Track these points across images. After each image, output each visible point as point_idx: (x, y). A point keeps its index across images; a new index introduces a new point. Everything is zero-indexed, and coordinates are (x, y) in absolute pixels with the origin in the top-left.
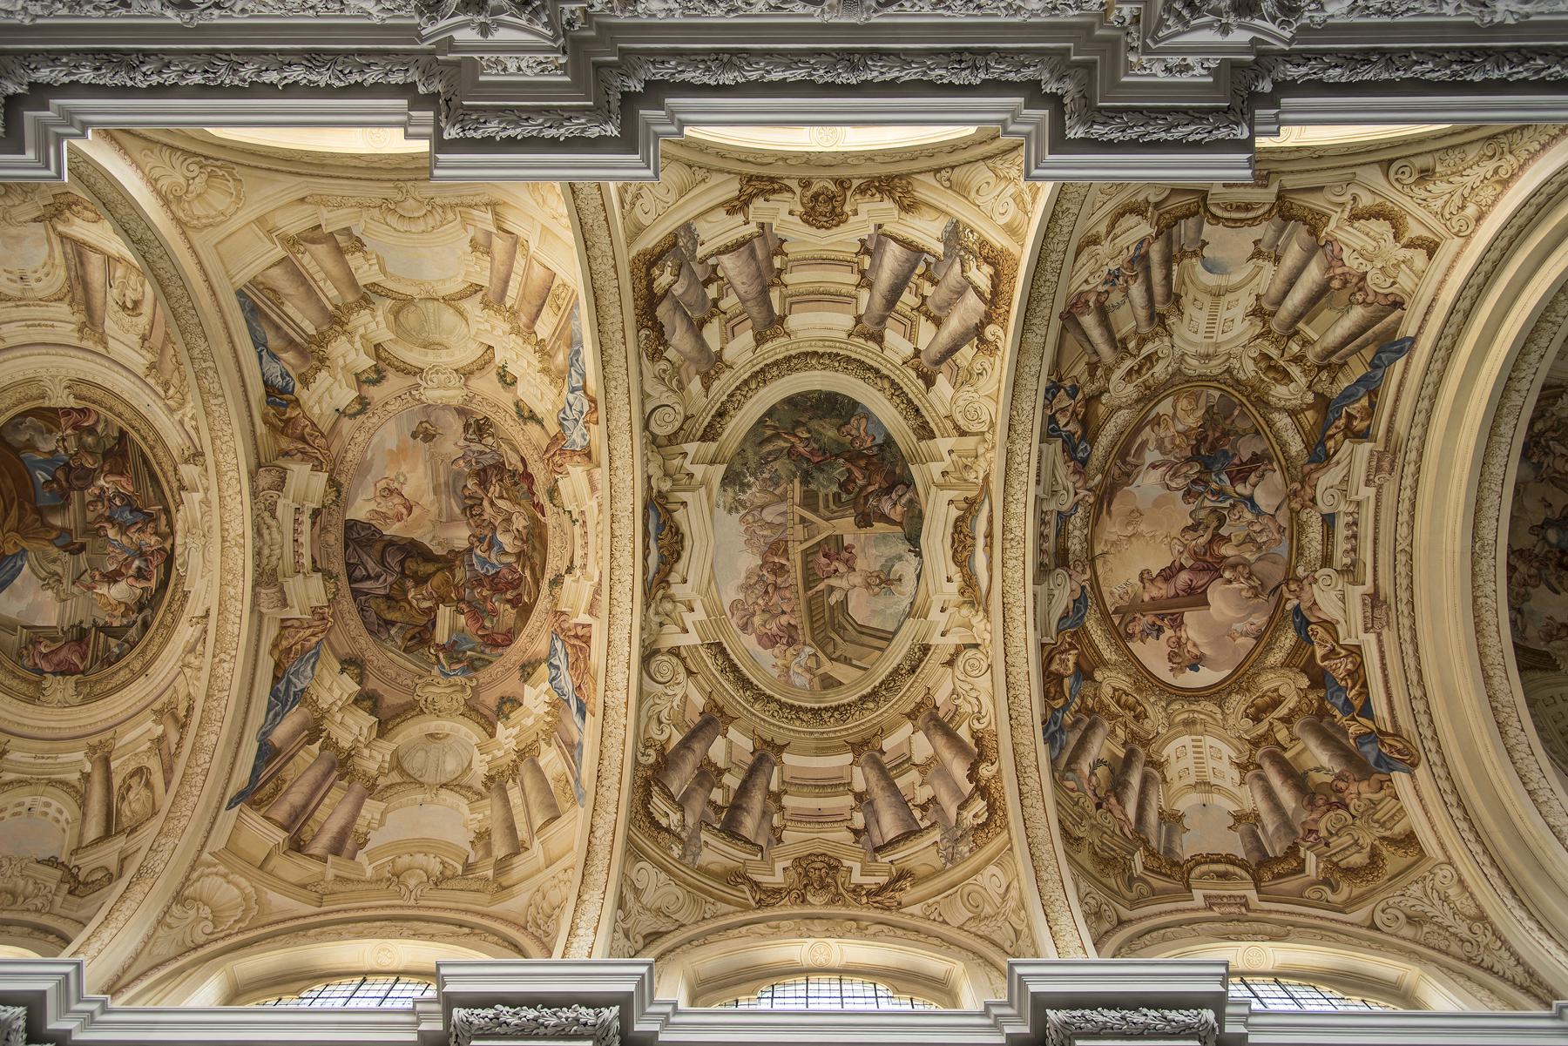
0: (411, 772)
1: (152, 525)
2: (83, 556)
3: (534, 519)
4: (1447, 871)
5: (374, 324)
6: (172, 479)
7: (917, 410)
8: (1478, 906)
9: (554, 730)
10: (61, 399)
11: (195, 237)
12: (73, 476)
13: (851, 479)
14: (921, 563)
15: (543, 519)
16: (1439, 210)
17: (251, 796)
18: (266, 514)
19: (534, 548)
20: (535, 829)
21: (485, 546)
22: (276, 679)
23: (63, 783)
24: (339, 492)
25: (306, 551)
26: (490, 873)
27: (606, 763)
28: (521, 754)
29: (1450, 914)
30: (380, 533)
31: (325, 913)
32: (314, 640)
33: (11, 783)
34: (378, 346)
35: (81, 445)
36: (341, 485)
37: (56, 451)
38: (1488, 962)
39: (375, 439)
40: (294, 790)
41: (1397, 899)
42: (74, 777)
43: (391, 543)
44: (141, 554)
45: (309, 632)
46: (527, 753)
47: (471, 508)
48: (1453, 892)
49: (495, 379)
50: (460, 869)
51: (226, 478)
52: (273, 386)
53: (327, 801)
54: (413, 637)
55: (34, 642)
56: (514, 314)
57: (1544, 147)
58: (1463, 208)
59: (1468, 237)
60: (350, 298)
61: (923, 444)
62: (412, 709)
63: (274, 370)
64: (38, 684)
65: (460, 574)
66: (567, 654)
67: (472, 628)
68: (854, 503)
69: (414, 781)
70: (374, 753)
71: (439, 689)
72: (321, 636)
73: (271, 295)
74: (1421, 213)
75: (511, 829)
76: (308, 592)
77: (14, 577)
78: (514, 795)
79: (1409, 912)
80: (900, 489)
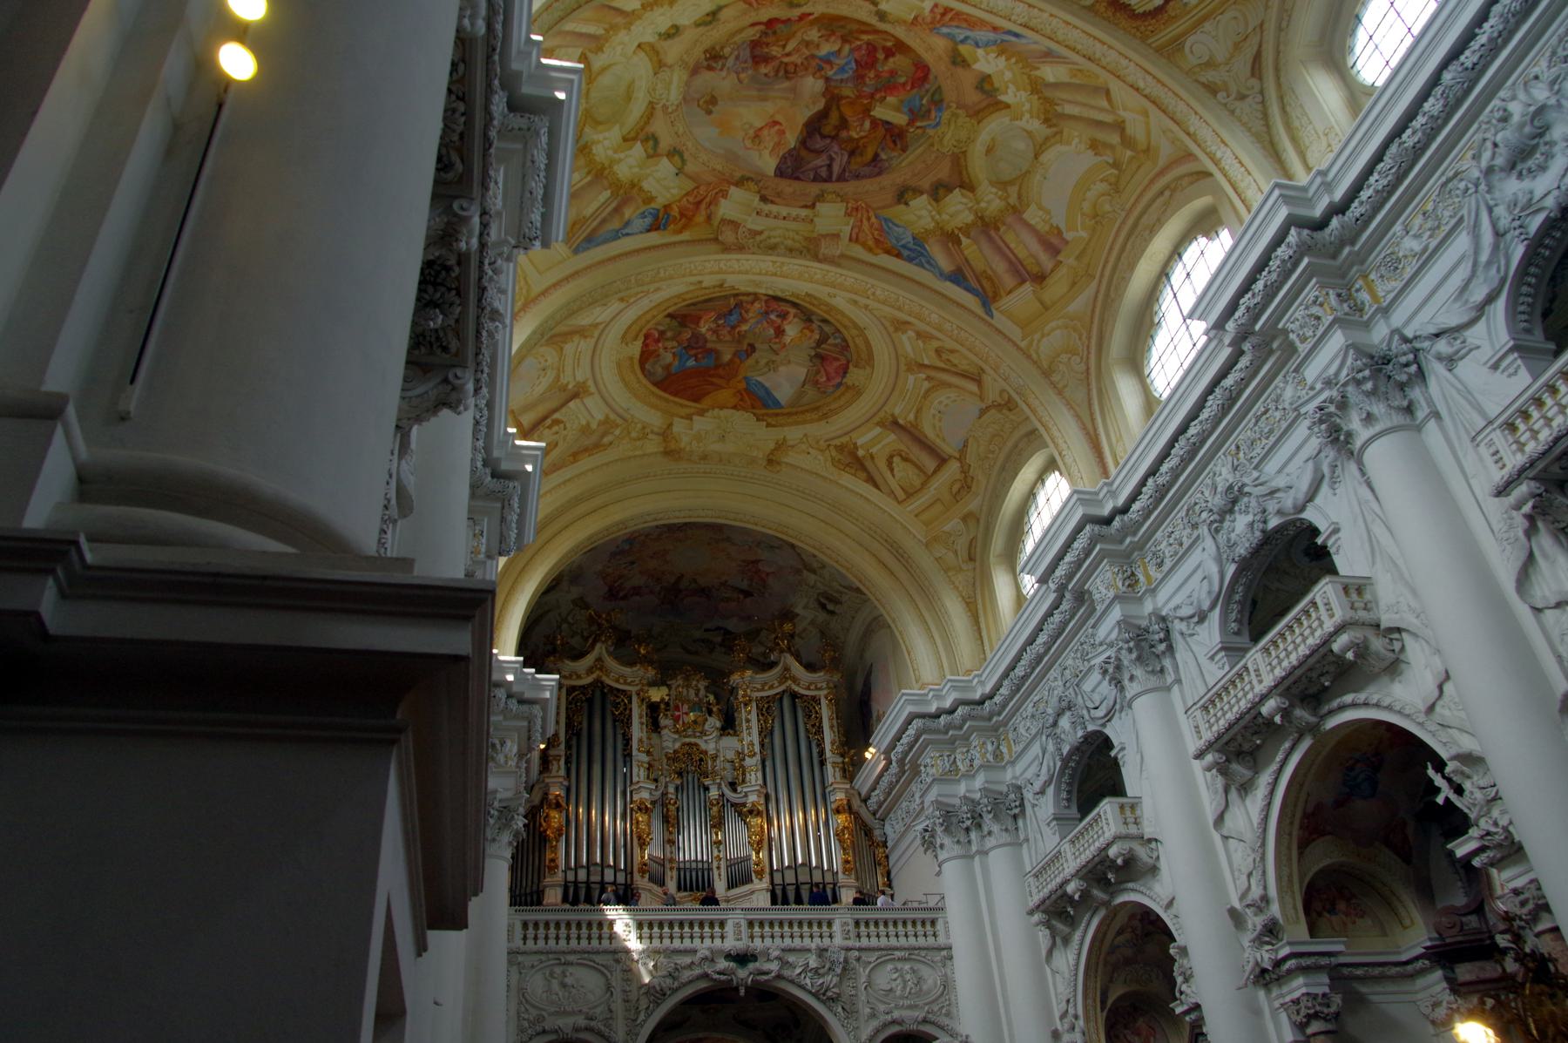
1: (744, 305)
2: (756, 345)
3: (812, 23)
6: (712, 290)
9: (1028, 62)
10: (636, 348)
11: (536, 290)
12: (696, 345)
15: (816, 15)
17: (989, 299)
18: (758, 238)
19: (842, 27)
21: (827, 67)
22: (899, 255)
23: (928, 391)
24: (748, 179)
25: (795, 212)
26: (1129, 153)
27: (1079, 47)
31: (1102, 275)
32: (873, 220)
33: (916, 418)
34: (625, 139)
35: (673, 339)
36: (743, 176)
37: (674, 353)
40: (994, 266)
42: (926, 385)
43: (803, 143)
44: (767, 313)
45: (865, 222)
46: (1037, 87)
47: (788, 72)
49: (669, 42)
50: (1115, 172)
51: (724, 268)
52: (651, 225)
53: (1012, 246)
54: (894, 142)
55: (817, 382)
56: (613, 28)
62: (958, 161)
63: (639, 224)
64: (848, 387)
65: (848, 91)
66: (958, 27)
70: (986, 199)
71: (949, 132)
72: (871, 214)
73: (577, 226)
75: (1099, 124)
76: (831, 216)
77: (763, 386)
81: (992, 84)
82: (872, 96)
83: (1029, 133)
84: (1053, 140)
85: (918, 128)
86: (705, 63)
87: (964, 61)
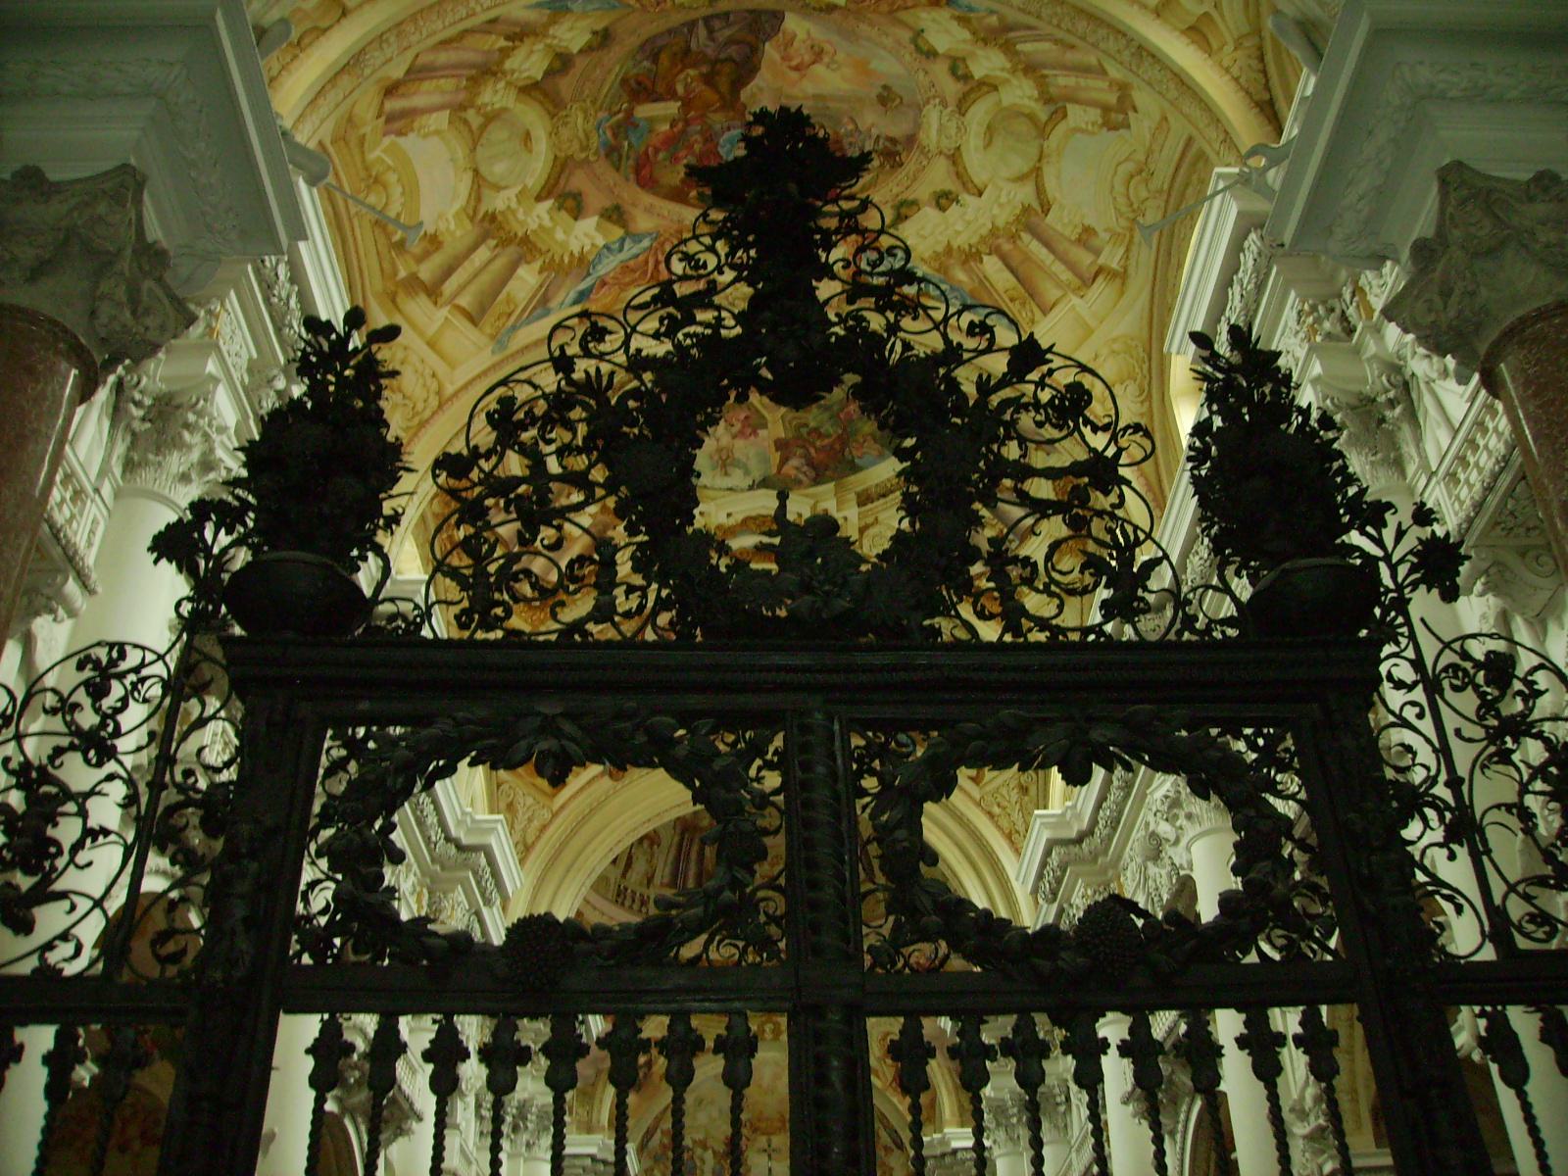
0: (485, 134)
4: (548, 815)
5: (1020, 93)
7: (884, 496)
13: (820, 436)
14: (742, 490)
20: (456, 301)
24: (821, 10)
26: (402, 274)
28: (526, 242)
30: (769, 38)
34: (995, 88)
39: (883, 53)
46: (526, 247)
48: (536, 824)
49: (950, 184)
53: (442, 81)
54: (639, 83)
59: (978, 804)
60: (1053, 90)
61: (852, 496)
66: (637, 256)
67: (655, 140)
68: (798, 437)
69: (475, 140)
70: (501, 93)
75: (448, 272)
78: (483, 254)
80: (813, 474)
81: (566, 209)
82: (687, 123)
83: (498, 188)
84: (472, 203)
85: (619, 111)
86: (899, 148)
87: (609, 218)
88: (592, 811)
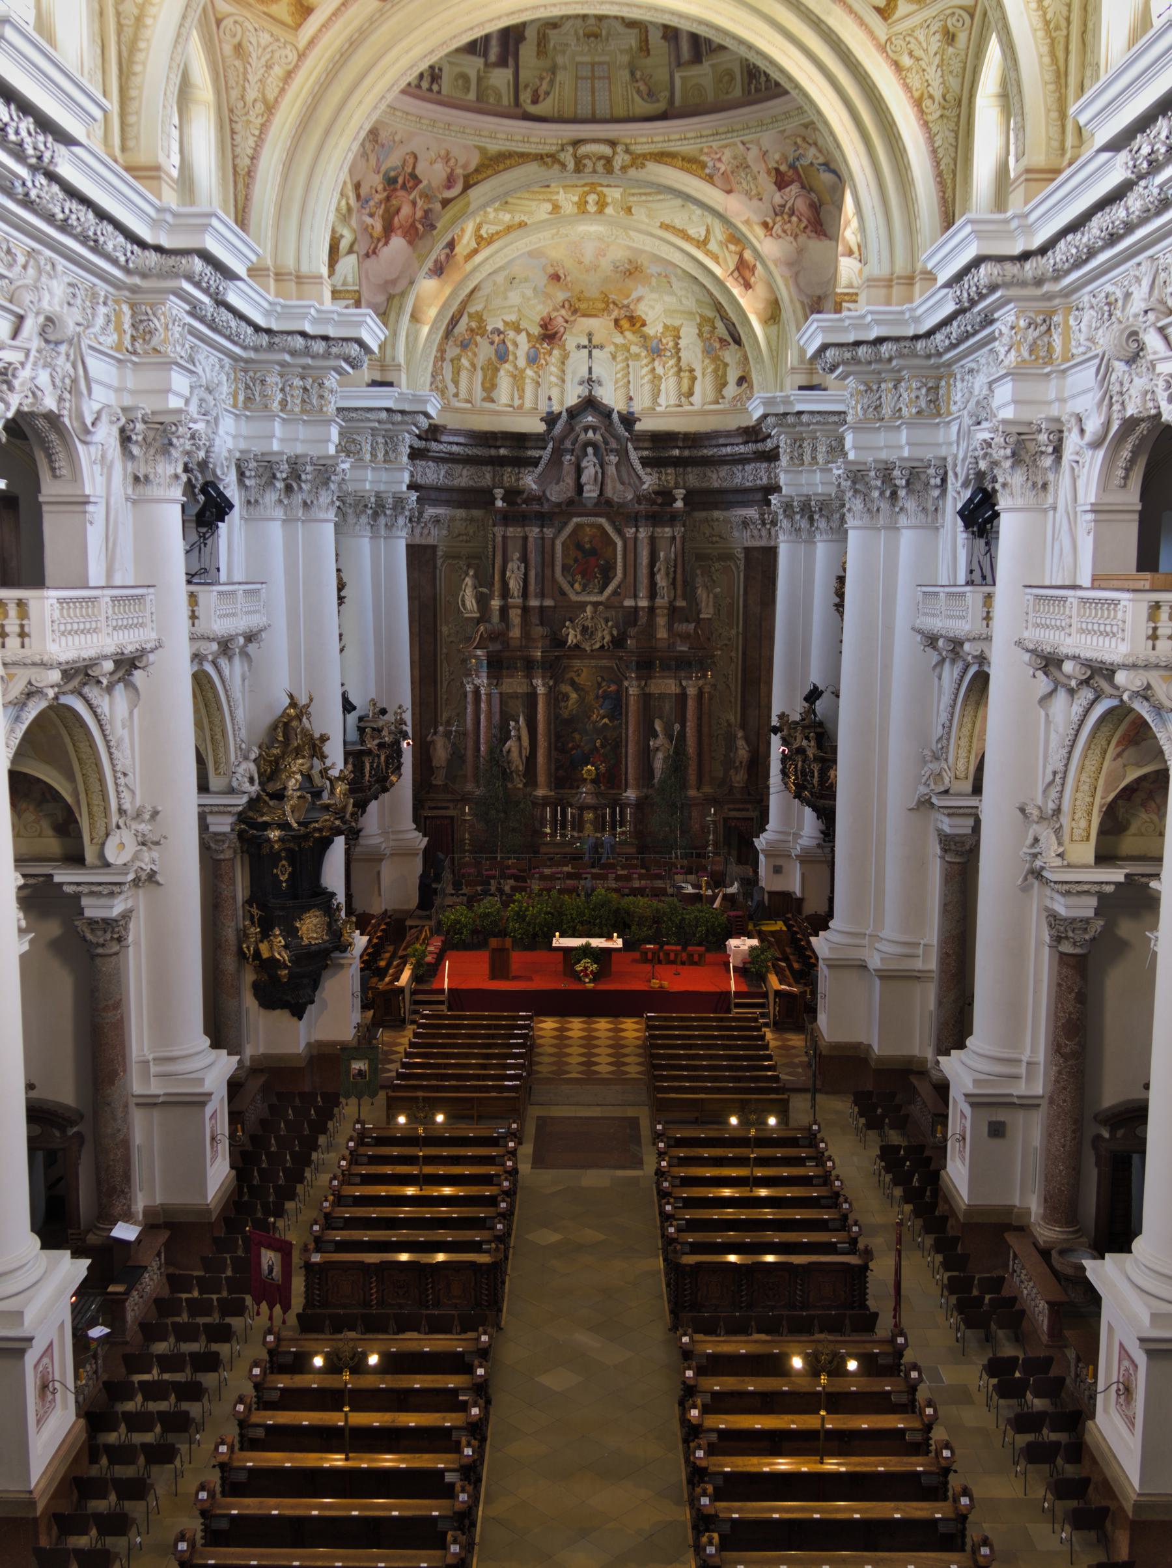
4: (293, 57)
8: (276, 100)
16: (915, 34)
29: (259, 76)
38: (238, 127)
41: (251, 28)
48: (278, 71)
57: (934, 151)
58: (911, 54)
59: (882, 48)
74: (918, 19)
79: (245, 43)
88: (353, 44)
